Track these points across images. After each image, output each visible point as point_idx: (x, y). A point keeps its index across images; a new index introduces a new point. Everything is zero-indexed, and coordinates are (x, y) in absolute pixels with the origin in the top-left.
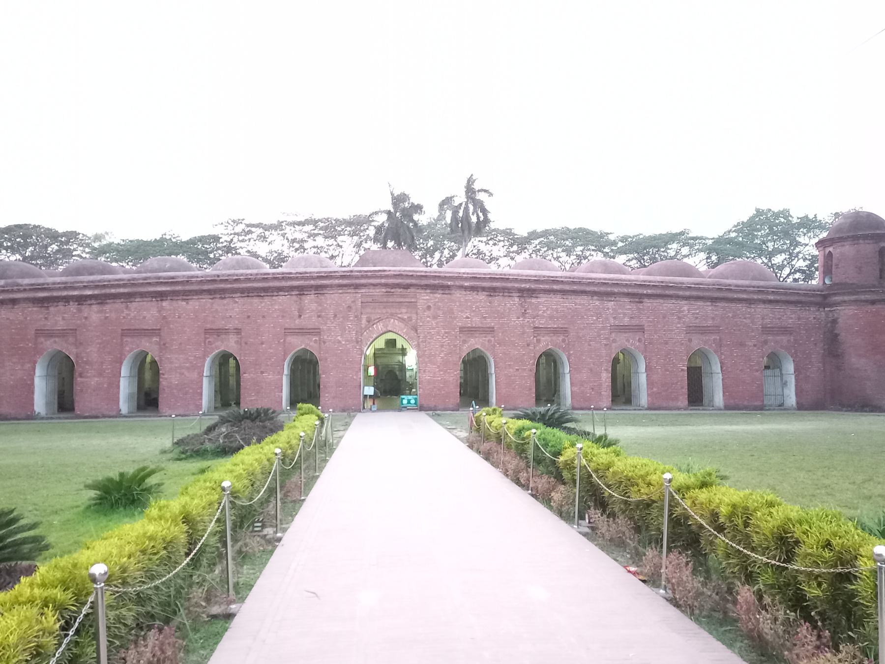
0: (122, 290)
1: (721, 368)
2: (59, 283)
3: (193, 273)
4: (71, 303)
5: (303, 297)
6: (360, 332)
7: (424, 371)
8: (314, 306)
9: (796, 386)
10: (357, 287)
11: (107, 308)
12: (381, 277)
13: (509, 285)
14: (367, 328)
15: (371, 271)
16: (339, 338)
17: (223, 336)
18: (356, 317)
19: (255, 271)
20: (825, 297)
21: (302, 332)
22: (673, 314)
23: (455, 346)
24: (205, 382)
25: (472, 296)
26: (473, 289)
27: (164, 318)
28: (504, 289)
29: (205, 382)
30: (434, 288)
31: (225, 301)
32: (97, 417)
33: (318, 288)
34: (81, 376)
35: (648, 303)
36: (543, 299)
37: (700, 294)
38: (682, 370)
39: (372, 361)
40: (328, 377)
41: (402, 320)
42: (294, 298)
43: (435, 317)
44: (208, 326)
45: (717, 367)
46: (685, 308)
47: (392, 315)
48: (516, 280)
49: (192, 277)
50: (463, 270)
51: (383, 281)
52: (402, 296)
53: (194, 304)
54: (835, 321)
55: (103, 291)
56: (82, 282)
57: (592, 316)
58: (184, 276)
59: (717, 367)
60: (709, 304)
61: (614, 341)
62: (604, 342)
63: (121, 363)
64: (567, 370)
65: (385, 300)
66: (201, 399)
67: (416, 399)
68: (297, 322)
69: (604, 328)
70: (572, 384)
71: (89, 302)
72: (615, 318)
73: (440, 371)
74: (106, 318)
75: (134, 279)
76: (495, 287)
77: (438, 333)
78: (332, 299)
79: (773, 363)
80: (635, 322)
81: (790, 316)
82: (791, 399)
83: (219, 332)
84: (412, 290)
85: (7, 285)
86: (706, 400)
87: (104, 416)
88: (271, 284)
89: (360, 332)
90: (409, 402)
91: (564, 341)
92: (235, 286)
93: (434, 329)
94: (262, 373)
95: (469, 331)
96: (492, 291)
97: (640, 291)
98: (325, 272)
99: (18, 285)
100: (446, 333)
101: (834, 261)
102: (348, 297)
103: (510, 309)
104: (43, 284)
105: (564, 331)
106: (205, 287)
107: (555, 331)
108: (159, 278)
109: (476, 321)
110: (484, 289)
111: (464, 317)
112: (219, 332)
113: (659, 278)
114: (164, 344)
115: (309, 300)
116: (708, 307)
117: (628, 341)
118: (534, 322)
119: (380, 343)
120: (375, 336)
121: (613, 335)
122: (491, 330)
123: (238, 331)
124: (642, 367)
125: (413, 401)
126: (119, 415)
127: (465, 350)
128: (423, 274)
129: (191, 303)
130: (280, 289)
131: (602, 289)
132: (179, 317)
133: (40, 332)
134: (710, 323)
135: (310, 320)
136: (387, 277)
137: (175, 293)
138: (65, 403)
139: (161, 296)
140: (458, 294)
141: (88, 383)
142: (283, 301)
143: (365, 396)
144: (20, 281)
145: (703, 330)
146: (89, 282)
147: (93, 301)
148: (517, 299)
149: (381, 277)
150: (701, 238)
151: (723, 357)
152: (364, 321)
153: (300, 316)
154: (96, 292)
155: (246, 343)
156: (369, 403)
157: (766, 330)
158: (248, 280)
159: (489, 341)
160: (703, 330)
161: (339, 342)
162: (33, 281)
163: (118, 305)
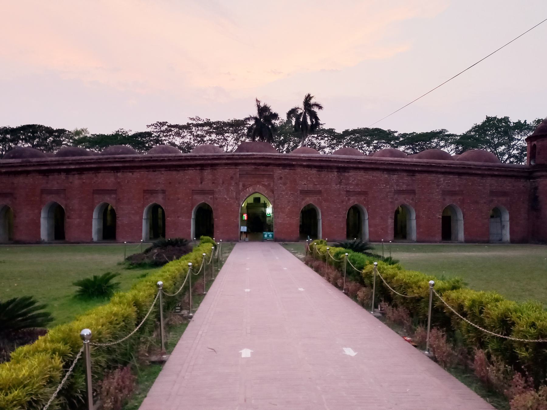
0: (93, 166)
1: (464, 216)
2: (55, 161)
3: (136, 155)
4: (62, 173)
5: (204, 171)
6: (238, 193)
7: (278, 217)
8: (210, 177)
9: (510, 228)
10: (237, 165)
11: (84, 176)
12: (252, 159)
13: (331, 164)
14: (243, 190)
15: (245, 155)
16: (225, 196)
17: (155, 195)
18: (236, 183)
19: (174, 155)
20: (531, 173)
21: (203, 192)
22: (434, 183)
23: (297, 202)
24: (144, 223)
25: (307, 171)
26: (308, 166)
27: (119, 183)
28: (328, 167)
29: (144, 223)
30: (284, 166)
31: (156, 173)
32: (78, 243)
33: (213, 166)
34: (69, 218)
35: (418, 176)
36: (352, 173)
37: (452, 171)
38: (439, 218)
39: (245, 211)
40: (219, 220)
41: (264, 185)
42: (198, 171)
43: (285, 184)
44: (146, 188)
45: (460, 216)
46: (442, 179)
47: (259, 183)
48: (335, 161)
49: (136, 158)
50: (302, 155)
51: (253, 161)
52: (264, 171)
53: (137, 175)
54: (536, 188)
55: (81, 166)
56: (68, 160)
57: (383, 184)
58: (130, 157)
59: (460, 216)
60: (457, 177)
61: (396, 200)
62: (390, 200)
63: (93, 211)
64: (367, 217)
65: (254, 173)
66: (141, 232)
67: (272, 235)
68: (200, 186)
69: (390, 192)
70: (370, 226)
71: (73, 173)
72: (397, 185)
73: (287, 217)
74: (84, 182)
75: (100, 159)
76: (323, 165)
77: (287, 194)
78: (221, 172)
79: (496, 214)
80: (410, 188)
81: (507, 185)
82: (507, 236)
83: (152, 192)
84: (270, 167)
85: (22, 162)
86: (453, 237)
87: (83, 243)
88: (184, 163)
89: (238, 193)
90: (268, 235)
91: (365, 199)
92: (162, 164)
93: (283, 191)
94: (178, 217)
95: (306, 193)
96: (320, 168)
97: (414, 168)
98: (217, 156)
99: (30, 162)
100: (292, 194)
101: (537, 151)
102: (231, 171)
103: (331, 179)
104: (45, 162)
105: (365, 193)
106: (144, 164)
107: (359, 193)
108: (115, 158)
109: (311, 187)
110: (315, 167)
111: (303, 185)
112: (152, 192)
113: (425, 160)
114: (119, 199)
115: (207, 173)
116: (456, 179)
117: (405, 199)
118: (346, 188)
119: (251, 200)
120: (247, 195)
121: (396, 196)
122: (319, 192)
123: (164, 192)
124: (414, 216)
125: (270, 236)
126: (92, 242)
127: (303, 205)
128: (278, 157)
129: (135, 174)
130: (189, 166)
131: (390, 167)
132: (128, 182)
133: (44, 191)
134: (457, 189)
135: (207, 185)
136: (255, 158)
137: (124, 168)
138: (59, 234)
140: (299, 170)
141: (73, 222)
142: (191, 172)
143: (241, 232)
144: (31, 159)
145: (453, 193)
146: (72, 160)
147: (75, 172)
148: (336, 173)
149: (252, 159)
150: (453, 135)
151: (465, 210)
152: (241, 186)
153: (201, 183)
154: (77, 167)
155: (169, 199)
156: (244, 237)
157: (493, 193)
158: (170, 160)
159: (318, 199)
160: (453, 193)
161: (226, 199)
162: (38, 160)
163: (90, 175)
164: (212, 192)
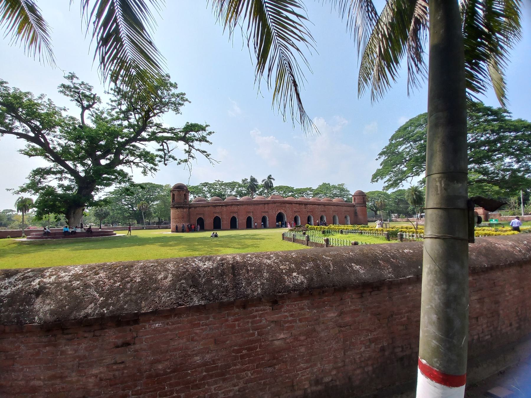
21: (265, 212)
78: (270, 205)
79: (346, 217)
81: (349, 209)
107: (311, 212)
115: (266, 205)
135: (266, 210)
139: (238, 205)
145: (335, 211)
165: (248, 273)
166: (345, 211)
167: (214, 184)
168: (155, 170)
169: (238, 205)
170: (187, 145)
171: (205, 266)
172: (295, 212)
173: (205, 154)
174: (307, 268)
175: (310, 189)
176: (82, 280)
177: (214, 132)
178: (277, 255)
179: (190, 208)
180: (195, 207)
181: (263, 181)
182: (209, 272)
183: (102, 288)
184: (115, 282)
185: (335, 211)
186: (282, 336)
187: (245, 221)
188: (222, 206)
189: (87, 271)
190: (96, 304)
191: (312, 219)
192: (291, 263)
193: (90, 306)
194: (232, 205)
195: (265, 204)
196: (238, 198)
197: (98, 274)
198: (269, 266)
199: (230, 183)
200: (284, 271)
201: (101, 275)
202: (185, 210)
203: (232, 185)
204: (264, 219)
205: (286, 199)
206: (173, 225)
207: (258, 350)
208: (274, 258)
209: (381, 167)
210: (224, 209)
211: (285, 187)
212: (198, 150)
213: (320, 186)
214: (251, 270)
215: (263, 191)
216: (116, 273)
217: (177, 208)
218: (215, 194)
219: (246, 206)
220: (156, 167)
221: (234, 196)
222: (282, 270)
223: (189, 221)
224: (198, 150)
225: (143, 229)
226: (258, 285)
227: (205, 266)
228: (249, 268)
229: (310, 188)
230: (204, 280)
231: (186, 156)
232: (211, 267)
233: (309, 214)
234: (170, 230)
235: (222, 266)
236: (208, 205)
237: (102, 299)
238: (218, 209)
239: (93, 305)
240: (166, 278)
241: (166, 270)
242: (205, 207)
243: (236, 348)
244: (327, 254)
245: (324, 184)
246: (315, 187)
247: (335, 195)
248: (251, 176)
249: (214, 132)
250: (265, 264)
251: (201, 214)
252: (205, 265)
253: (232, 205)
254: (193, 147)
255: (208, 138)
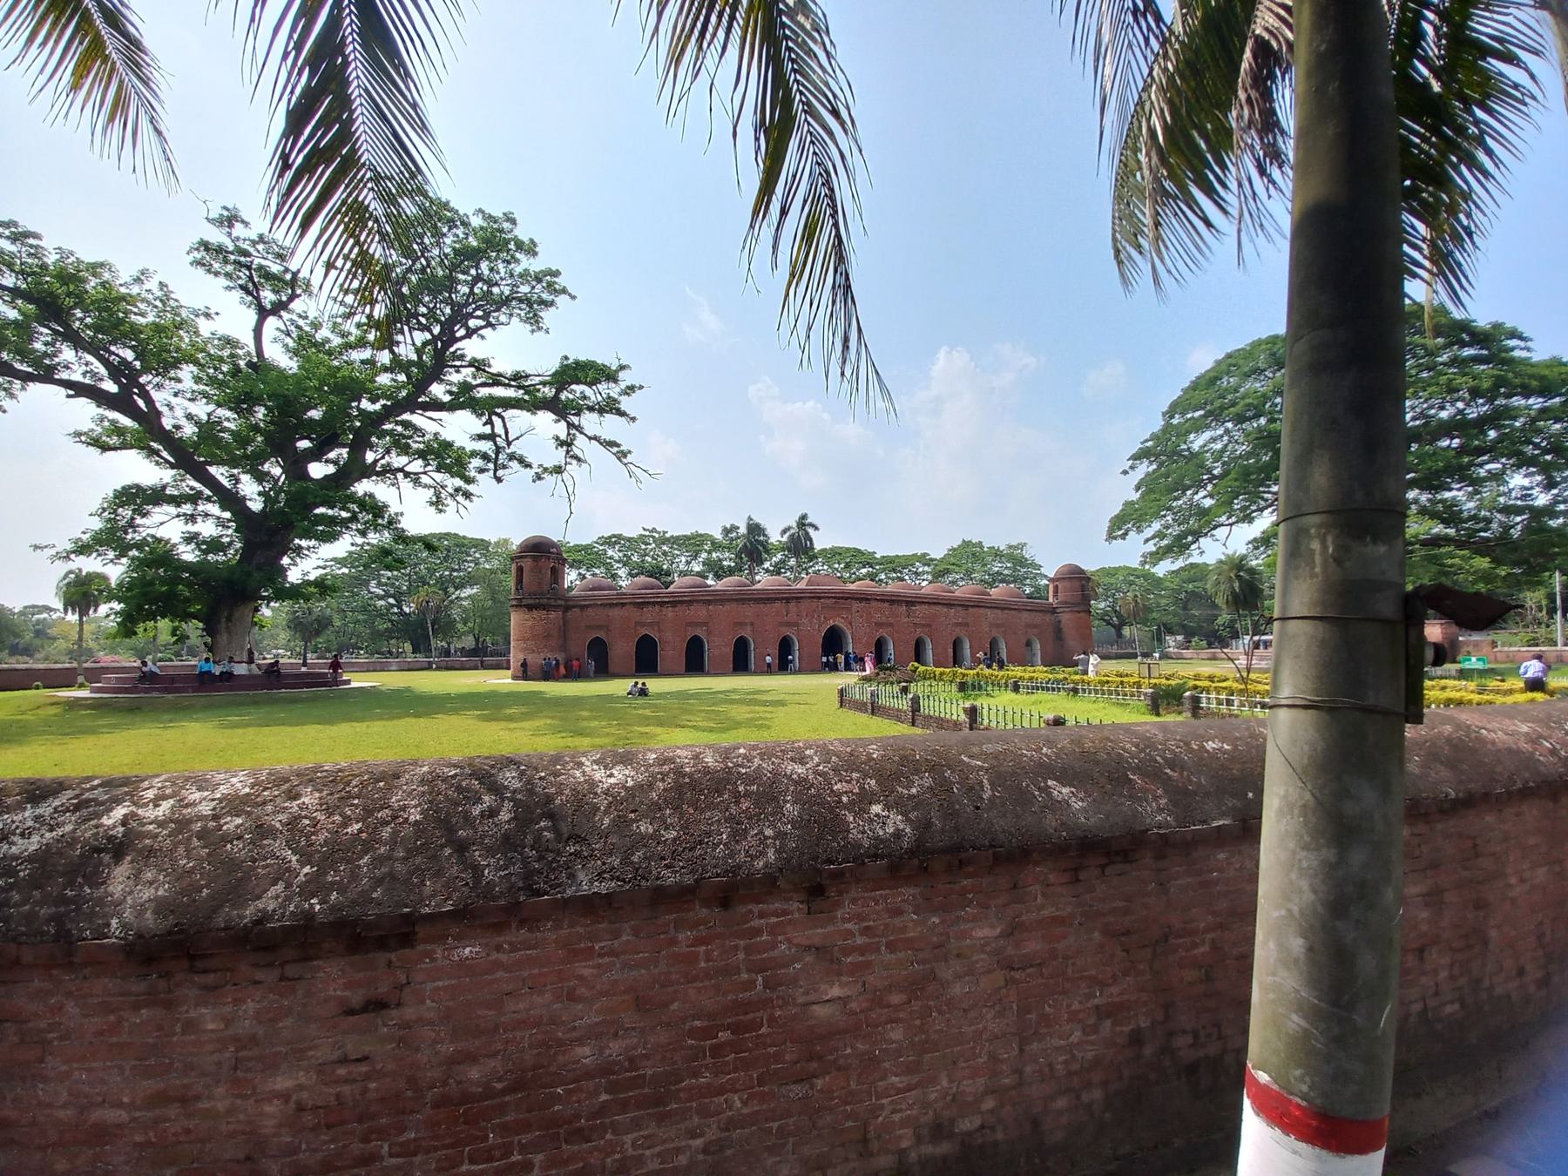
21: (788, 624)
25: (880, 605)
30: (861, 600)
78: (805, 604)
79: (1029, 644)
105: (929, 626)
135: (792, 617)
139: (708, 602)
140: (874, 604)
145: (997, 626)
164: (797, 625)
165: (737, 803)
166: (1028, 626)
167: (642, 539)
168: (468, 495)
169: (708, 602)
170: (563, 424)
171: (612, 780)
172: (879, 625)
173: (615, 450)
174: (914, 791)
175: (924, 559)
176: (249, 814)
177: (641, 387)
178: (824, 751)
179: (567, 609)
180: (583, 607)
181: (784, 532)
182: (627, 801)
183: (308, 837)
184: (347, 821)
185: (997, 626)
186: (836, 991)
187: (729, 650)
188: (662, 604)
189: (266, 789)
190: (288, 886)
191: (929, 646)
192: (866, 776)
193: (273, 891)
194: (690, 603)
195: (788, 600)
196: (710, 582)
197: (297, 797)
198: (801, 781)
199: (687, 538)
200: (845, 799)
201: (306, 800)
202: (553, 615)
203: (693, 543)
204: (785, 647)
205: (852, 587)
206: (515, 657)
207: (763, 1030)
208: (816, 759)
209: (1135, 496)
210: (669, 612)
211: (848, 549)
212: (595, 438)
213: (954, 550)
214: (747, 794)
215: (783, 562)
216: (350, 796)
217: (530, 608)
218: (640, 570)
219: (734, 605)
220: (471, 488)
221: (699, 574)
222: (839, 795)
223: (563, 647)
224: (595, 438)
225: (429, 667)
226: (766, 838)
227: (612, 780)
228: (741, 788)
229: (925, 555)
230: (606, 821)
231: (559, 456)
232: (630, 783)
233: (919, 632)
234: (509, 673)
235: (663, 780)
236: (621, 601)
237: (307, 869)
238: (649, 614)
239: (280, 887)
240: (492, 813)
241: (496, 789)
242: (611, 605)
243: (697, 1023)
244: (975, 750)
245: (966, 544)
246: (938, 553)
247: (998, 578)
248: (750, 518)
249: (641, 387)
250: (789, 777)
251: (600, 627)
252: (611, 775)
253: (690, 603)
254: (579, 428)
255: (625, 404)
